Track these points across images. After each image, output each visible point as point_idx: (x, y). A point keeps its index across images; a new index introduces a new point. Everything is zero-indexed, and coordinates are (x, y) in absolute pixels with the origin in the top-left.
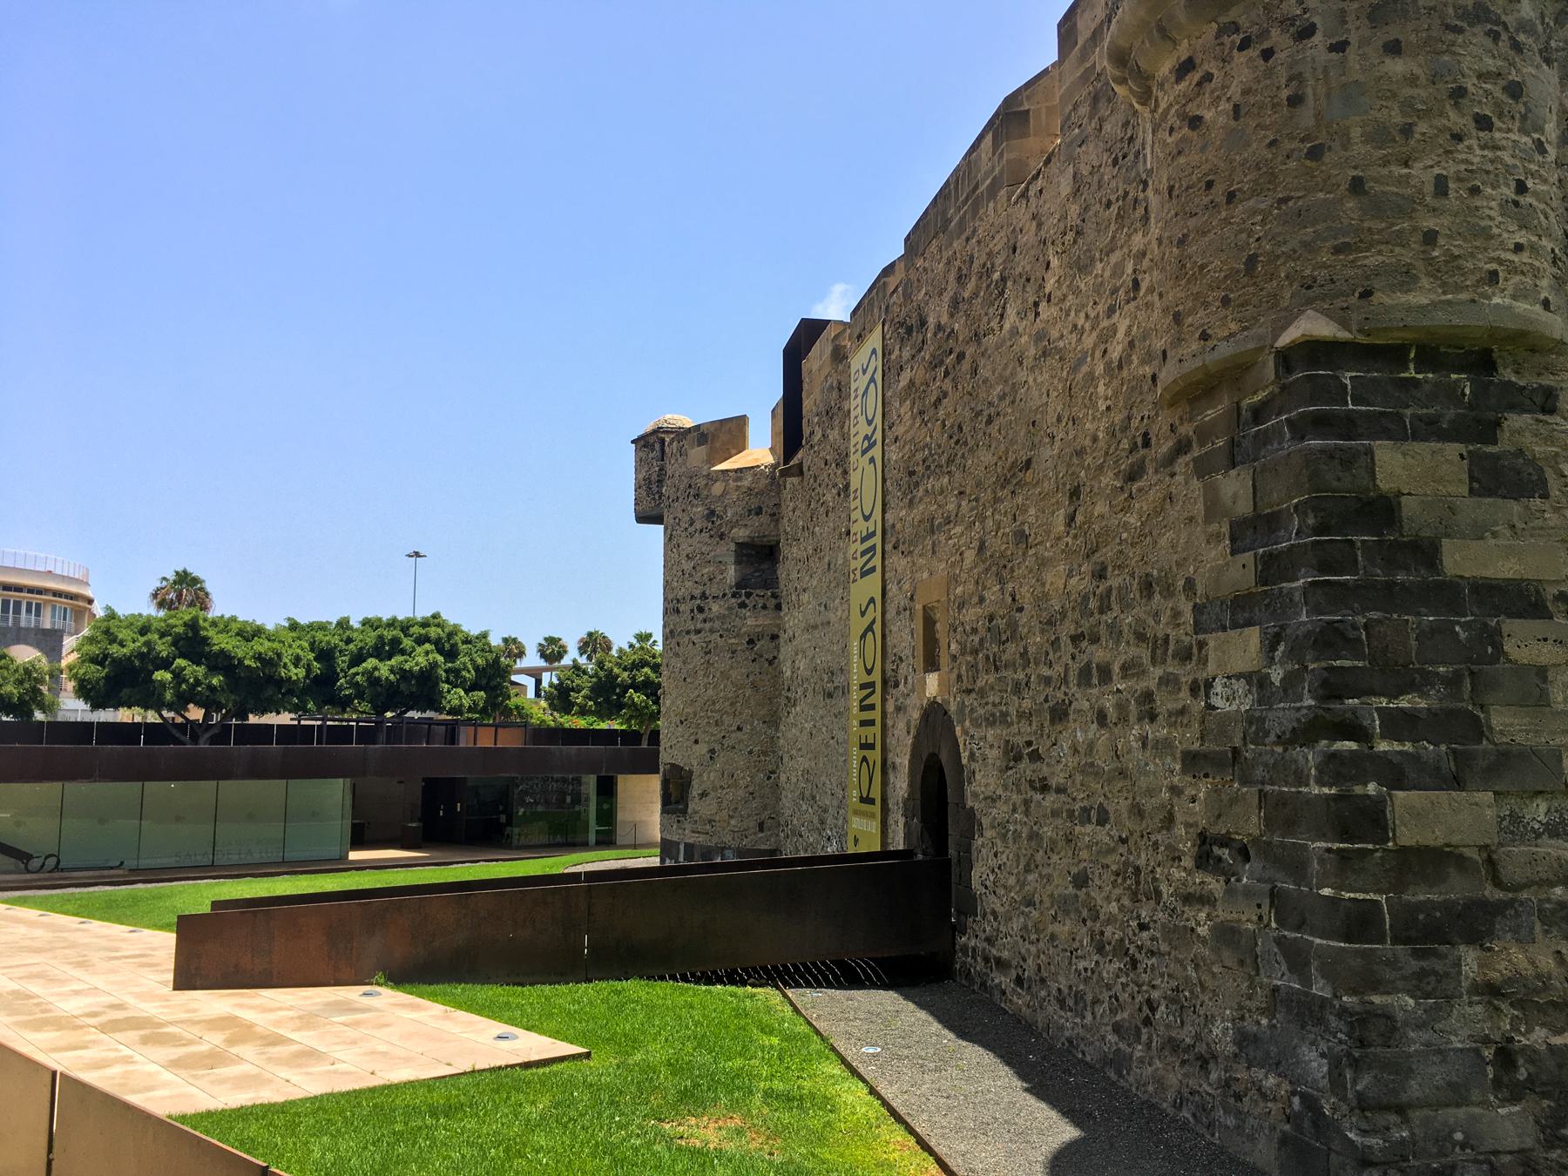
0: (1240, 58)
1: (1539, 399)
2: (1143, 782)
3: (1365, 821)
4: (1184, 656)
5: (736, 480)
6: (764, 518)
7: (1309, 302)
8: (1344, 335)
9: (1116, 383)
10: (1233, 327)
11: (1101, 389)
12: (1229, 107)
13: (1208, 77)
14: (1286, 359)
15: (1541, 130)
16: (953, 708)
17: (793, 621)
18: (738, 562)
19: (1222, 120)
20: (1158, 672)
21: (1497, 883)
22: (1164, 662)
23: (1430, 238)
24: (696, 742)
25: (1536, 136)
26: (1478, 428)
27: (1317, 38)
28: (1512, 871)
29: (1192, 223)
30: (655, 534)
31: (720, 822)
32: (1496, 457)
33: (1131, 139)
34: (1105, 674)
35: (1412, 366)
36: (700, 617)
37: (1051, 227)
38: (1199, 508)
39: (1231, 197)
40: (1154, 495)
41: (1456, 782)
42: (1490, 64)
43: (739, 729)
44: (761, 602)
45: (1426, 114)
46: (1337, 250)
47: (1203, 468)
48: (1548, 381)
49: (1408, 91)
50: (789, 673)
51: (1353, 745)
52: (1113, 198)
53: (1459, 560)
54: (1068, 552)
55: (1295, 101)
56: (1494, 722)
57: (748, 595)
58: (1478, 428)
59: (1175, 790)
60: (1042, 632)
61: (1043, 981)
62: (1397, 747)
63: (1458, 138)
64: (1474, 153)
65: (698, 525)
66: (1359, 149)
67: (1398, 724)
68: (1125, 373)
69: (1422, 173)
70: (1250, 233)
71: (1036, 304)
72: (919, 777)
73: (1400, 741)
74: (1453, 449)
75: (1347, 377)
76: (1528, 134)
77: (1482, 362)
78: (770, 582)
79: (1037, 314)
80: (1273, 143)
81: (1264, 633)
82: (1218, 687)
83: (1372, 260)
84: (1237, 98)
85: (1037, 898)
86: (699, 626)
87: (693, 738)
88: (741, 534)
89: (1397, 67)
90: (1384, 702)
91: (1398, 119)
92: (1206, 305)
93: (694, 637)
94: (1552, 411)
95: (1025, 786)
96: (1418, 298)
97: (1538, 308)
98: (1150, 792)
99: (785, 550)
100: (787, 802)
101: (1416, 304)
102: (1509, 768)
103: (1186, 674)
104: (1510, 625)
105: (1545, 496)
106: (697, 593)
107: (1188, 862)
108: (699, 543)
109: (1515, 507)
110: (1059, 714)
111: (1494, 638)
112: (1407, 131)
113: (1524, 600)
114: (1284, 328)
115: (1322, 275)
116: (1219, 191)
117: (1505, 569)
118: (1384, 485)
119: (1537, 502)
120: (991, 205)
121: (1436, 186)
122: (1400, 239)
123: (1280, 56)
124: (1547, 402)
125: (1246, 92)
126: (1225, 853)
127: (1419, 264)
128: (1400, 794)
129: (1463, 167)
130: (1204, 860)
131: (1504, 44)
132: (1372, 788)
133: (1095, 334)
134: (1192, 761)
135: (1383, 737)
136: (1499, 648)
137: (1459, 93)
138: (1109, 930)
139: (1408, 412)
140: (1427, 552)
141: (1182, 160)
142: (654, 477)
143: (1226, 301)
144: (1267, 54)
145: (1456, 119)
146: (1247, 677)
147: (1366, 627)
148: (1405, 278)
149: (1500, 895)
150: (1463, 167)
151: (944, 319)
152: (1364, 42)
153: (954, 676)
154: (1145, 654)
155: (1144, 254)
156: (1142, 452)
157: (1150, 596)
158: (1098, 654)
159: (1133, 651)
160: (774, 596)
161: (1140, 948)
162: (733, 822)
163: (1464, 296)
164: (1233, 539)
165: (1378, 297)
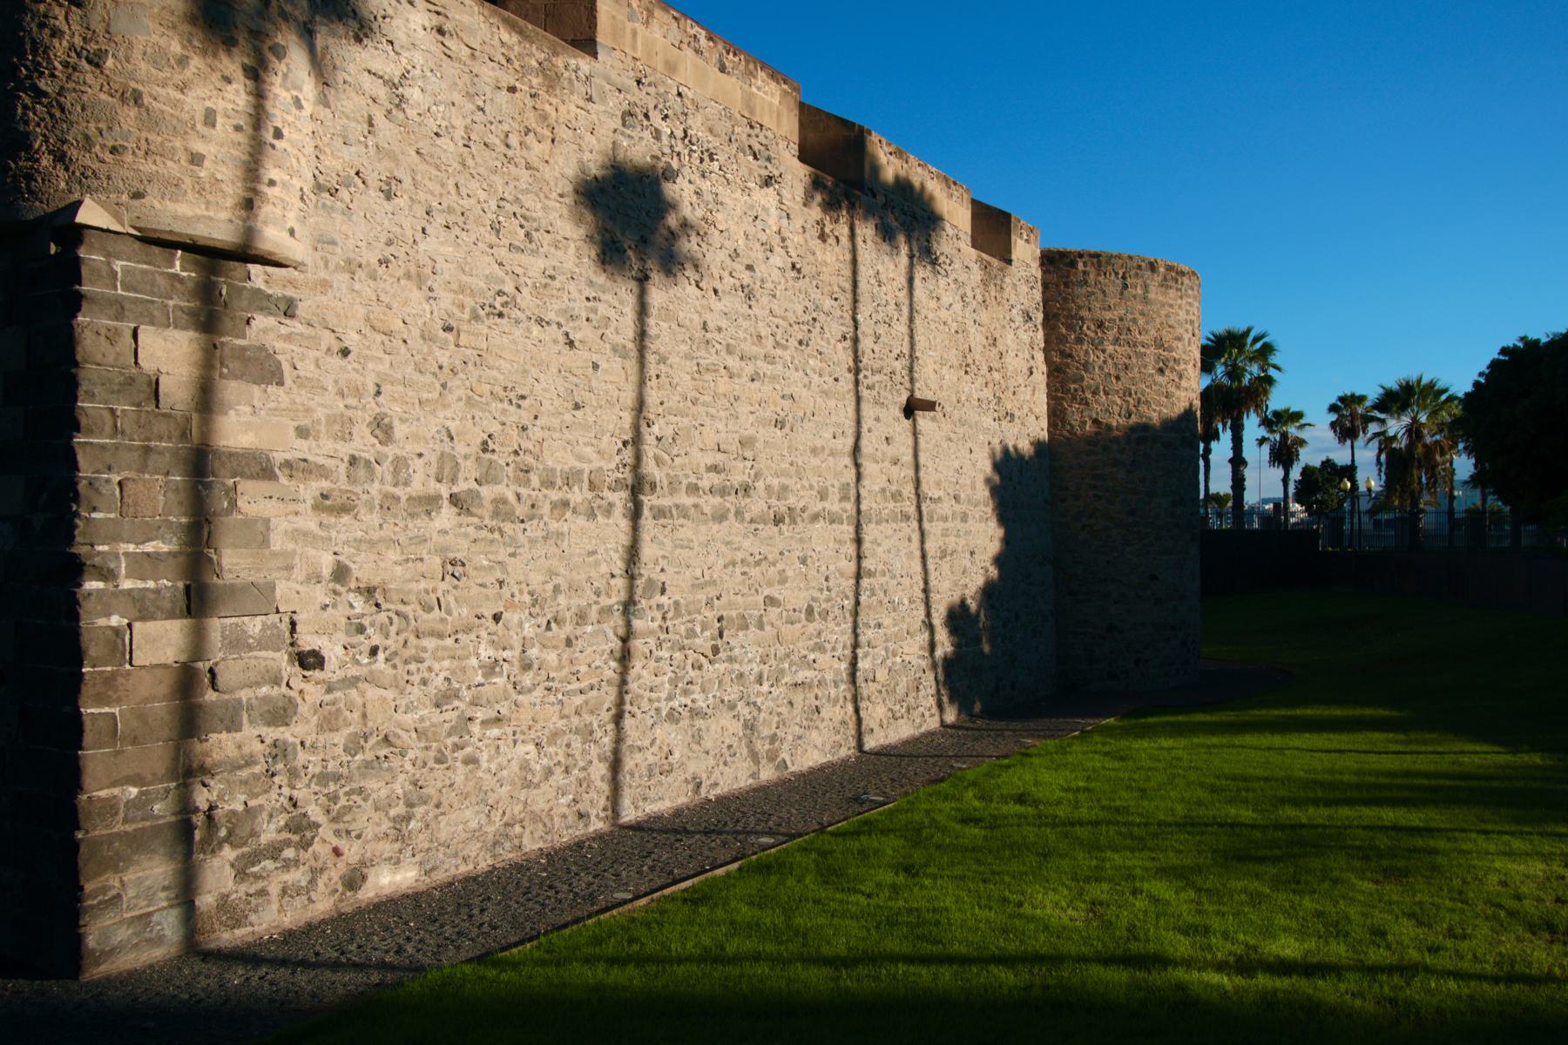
1: (283, 307)
15: (300, 89)
23: (196, 159)
25: (295, 93)
32: (243, 349)
35: (178, 263)
48: (290, 292)
62: (140, 585)
73: (143, 579)
75: (118, 265)
76: (288, 90)
90: (131, 548)
94: (292, 316)
96: (183, 209)
97: (286, 235)
105: (281, 383)
109: (256, 390)
119: (272, 389)
121: (206, 117)
127: (188, 180)
129: (230, 106)
132: (115, 620)
135: (127, 577)
136: (233, 503)
139: (171, 303)
147: (120, 483)
148: (173, 188)
150: (230, 106)
165: (152, 200)
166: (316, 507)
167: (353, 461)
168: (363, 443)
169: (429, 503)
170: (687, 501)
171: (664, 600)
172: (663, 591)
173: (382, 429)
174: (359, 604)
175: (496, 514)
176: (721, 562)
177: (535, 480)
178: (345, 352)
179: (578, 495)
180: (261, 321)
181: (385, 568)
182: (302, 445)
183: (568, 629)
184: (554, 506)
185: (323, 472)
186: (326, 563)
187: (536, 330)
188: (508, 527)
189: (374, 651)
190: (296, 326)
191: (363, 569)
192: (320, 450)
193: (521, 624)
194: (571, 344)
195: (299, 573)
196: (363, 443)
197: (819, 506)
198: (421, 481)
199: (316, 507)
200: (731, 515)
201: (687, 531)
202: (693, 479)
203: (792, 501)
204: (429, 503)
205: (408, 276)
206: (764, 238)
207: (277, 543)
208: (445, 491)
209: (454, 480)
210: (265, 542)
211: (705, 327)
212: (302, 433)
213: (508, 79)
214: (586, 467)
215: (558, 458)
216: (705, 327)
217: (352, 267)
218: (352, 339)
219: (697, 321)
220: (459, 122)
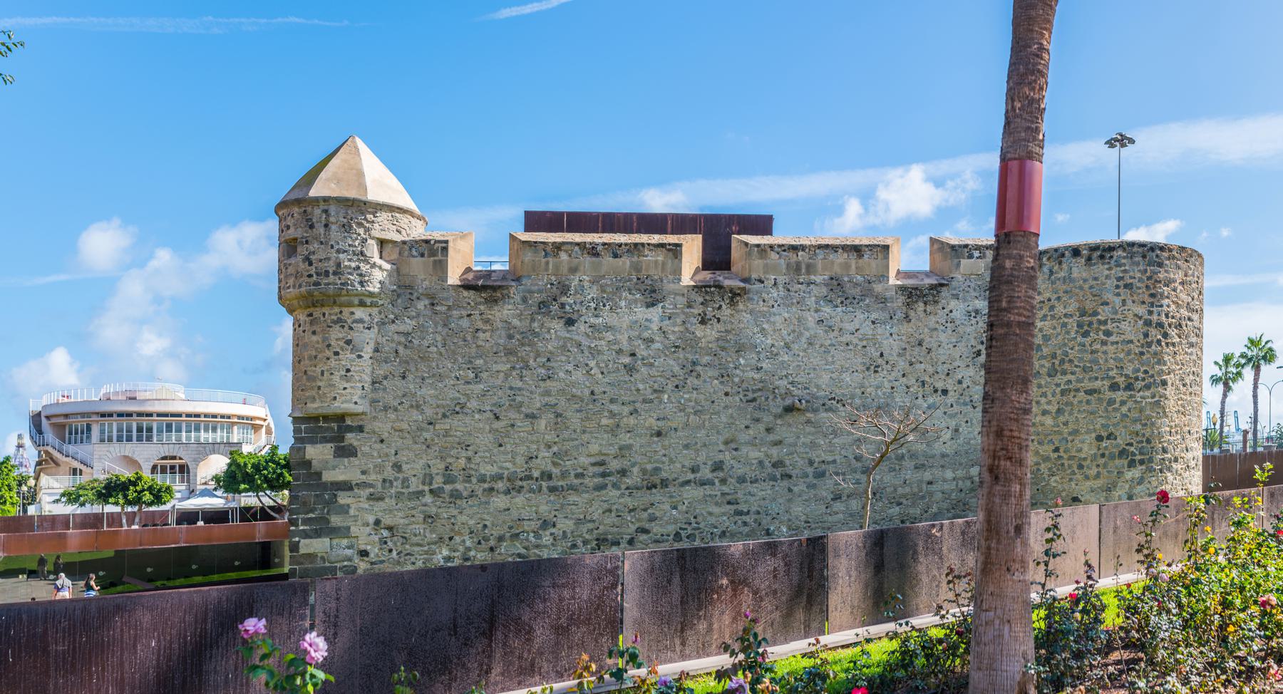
23: (319, 388)
41: (319, 536)
53: (328, 477)
64: (333, 363)
67: (305, 522)
69: (318, 370)
77: (341, 418)
89: (314, 338)
91: (314, 353)
96: (315, 405)
102: (334, 532)
104: (340, 493)
113: (346, 486)
118: (307, 457)
122: (312, 388)
124: (360, 429)
145: (329, 353)
148: (314, 399)
166: (368, 499)
167: (384, 481)
168: (389, 472)
169: (421, 493)
170: (577, 482)
171: (553, 530)
172: (554, 526)
173: (397, 467)
174: (385, 533)
175: (451, 496)
176: (600, 511)
177: (474, 480)
178: (382, 441)
179: (500, 485)
180: (349, 435)
181: (398, 519)
182: (364, 477)
183: (492, 543)
184: (484, 490)
185: (371, 486)
186: (371, 519)
187: (477, 416)
188: (458, 502)
189: (391, 551)
190: (365, 435)
191: (387, 520)
192: (372, 478)
193: (464, 541)
194: (497, 418)
195: (359, 523)
196: (389, 472)
197: (691, 476)
198: (415, 485)
199: (368, 499)
200: (609, 486)
201: (573, 498)
202: (580, 471)
203: (664, 475)
204: (420, 494)
205: (412, 406)
206: (646, 335)
207: (352, 512)
208: (426, 488)
209: (431, 484)
210: (347, 512)
211: (592, 393)
212: (363, 473)
213: (464, 313)
214: (506, 473)
215: (488, 470)
216: (592, 393)
217: (386, 408)
218: (385, 436)
219: (587, 392)
220: (439, 338)
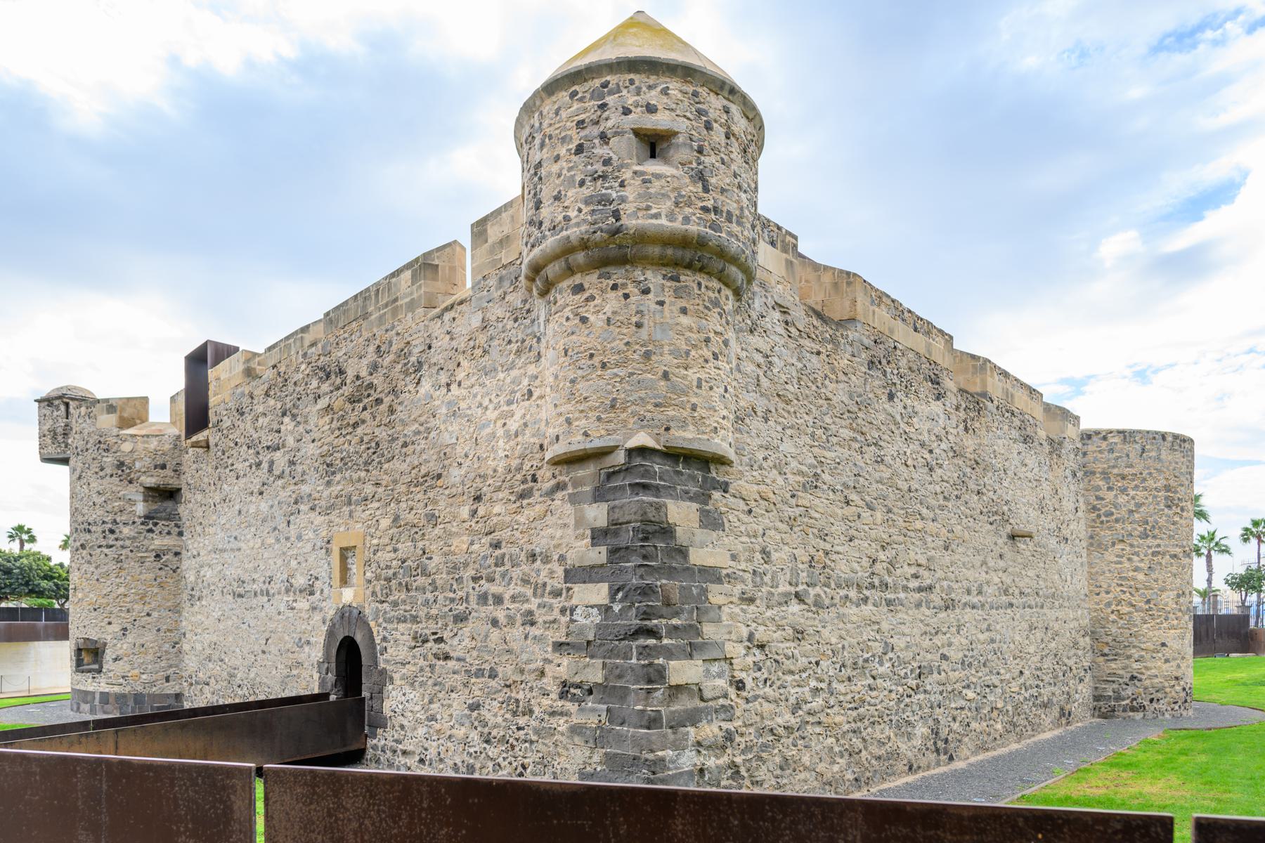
0: (612, 295)
2: (524, 657)
3: (655, 676)
4: (557, 594)
5: (144, 442)
6: (169, 472)
7: (643, 427)
8: (658, 447)
9: (512, 443)
10: (603, 432)
11: (501, 443)
12: (605, 317)
13: (592, 298)
14: (630, 452)
16: (367, 611)
17: (192, 544)
18: (145, 501)
19: (600, 324)
20: (538, 601)
21: (702, 699)
22: (542, 596)
24: (110, 623)
26: (703, 498)
27: (651, 296)
28: (708, 694)
29: (580, 372)
30: (62, 473)
31: (126, 675)
33: (528, 311)
34: (499, 600)
36: (113, 537)
37: (461, 343)
38: (571, 521)
39: (604, 366)
40: (539, 509)
42: (719, 329)
43: (148, 615)
44: (166, 529)
45: (694, 346)
46: (656, 405)
47: (573, 499)
49: (688, 334)
50: (192, 578)
51: (654, 641)
52: (514, 340)
54: (470, 530)
55: (639, 325)
56: (704, 630)
57: (155, 524)
58: (703, 498)
59: (547, 661)
60: (448, 573)
61: (441, 760)
63: (706, 361)
65: (108, 471)
66: (668, 358)
68: (520, 439)
69: (693, 375)
70: (614, 387)
71: (448, 385)
72: (334, 651)
74: (695, 506)
78: (173, 517)
79: (449, 390)
80: (627, 344)
81: (610, 588)
82: (578, 611)
83: (671, 412)
84: (609, 314)
85: (439, 717)
86: (111, 543)
87: (107, 620)
88: (150, 481)
89: (685, 320)
91: (684, 347)
92: (587, 418)
93: (106, 551)
95: (430, 656)
96: (689, 435)
98: (529, 662)
99: (186, 493)
100: (191, 663)
101: (686, 437)
103: (557, 603)
106: (109, 519)
107: (554, 696)
108: (111, 484)
110: (461, 619)
111: (705, 591)
112: (687, 353)
114: (629, 439)
115: (649, 415)
116: (596, 360)
117: (710, 562)
120: (410, 315)
123: (632, 299)
125: (614, 313)
126: (578, 691)
128: (672, 663)
130: (563, 695)
131: (724, 320)
133: (496, 413)
134: (559, 646)
137: (707, 340)
138: (494, 733)
140: (682, 552)
141: (574, 337)
142: (60, 430)
143: (599, 419)
144: (626, 296)
146: (599, 607)
148: (684, 425)
149: (703, 704)
151: (364, 373)
152: (672, 304)
153: (368, 592)
154: (529, 592)
155: (537, 377)
156: (531, 484)
157: (534, 561)
158: (494, 589)
159: (519, 589)
160: (177, 526)
161: (517, 740)
162: (144, 677)
163: (705, 437)
164: (593, 538)
165: (672, 431)
